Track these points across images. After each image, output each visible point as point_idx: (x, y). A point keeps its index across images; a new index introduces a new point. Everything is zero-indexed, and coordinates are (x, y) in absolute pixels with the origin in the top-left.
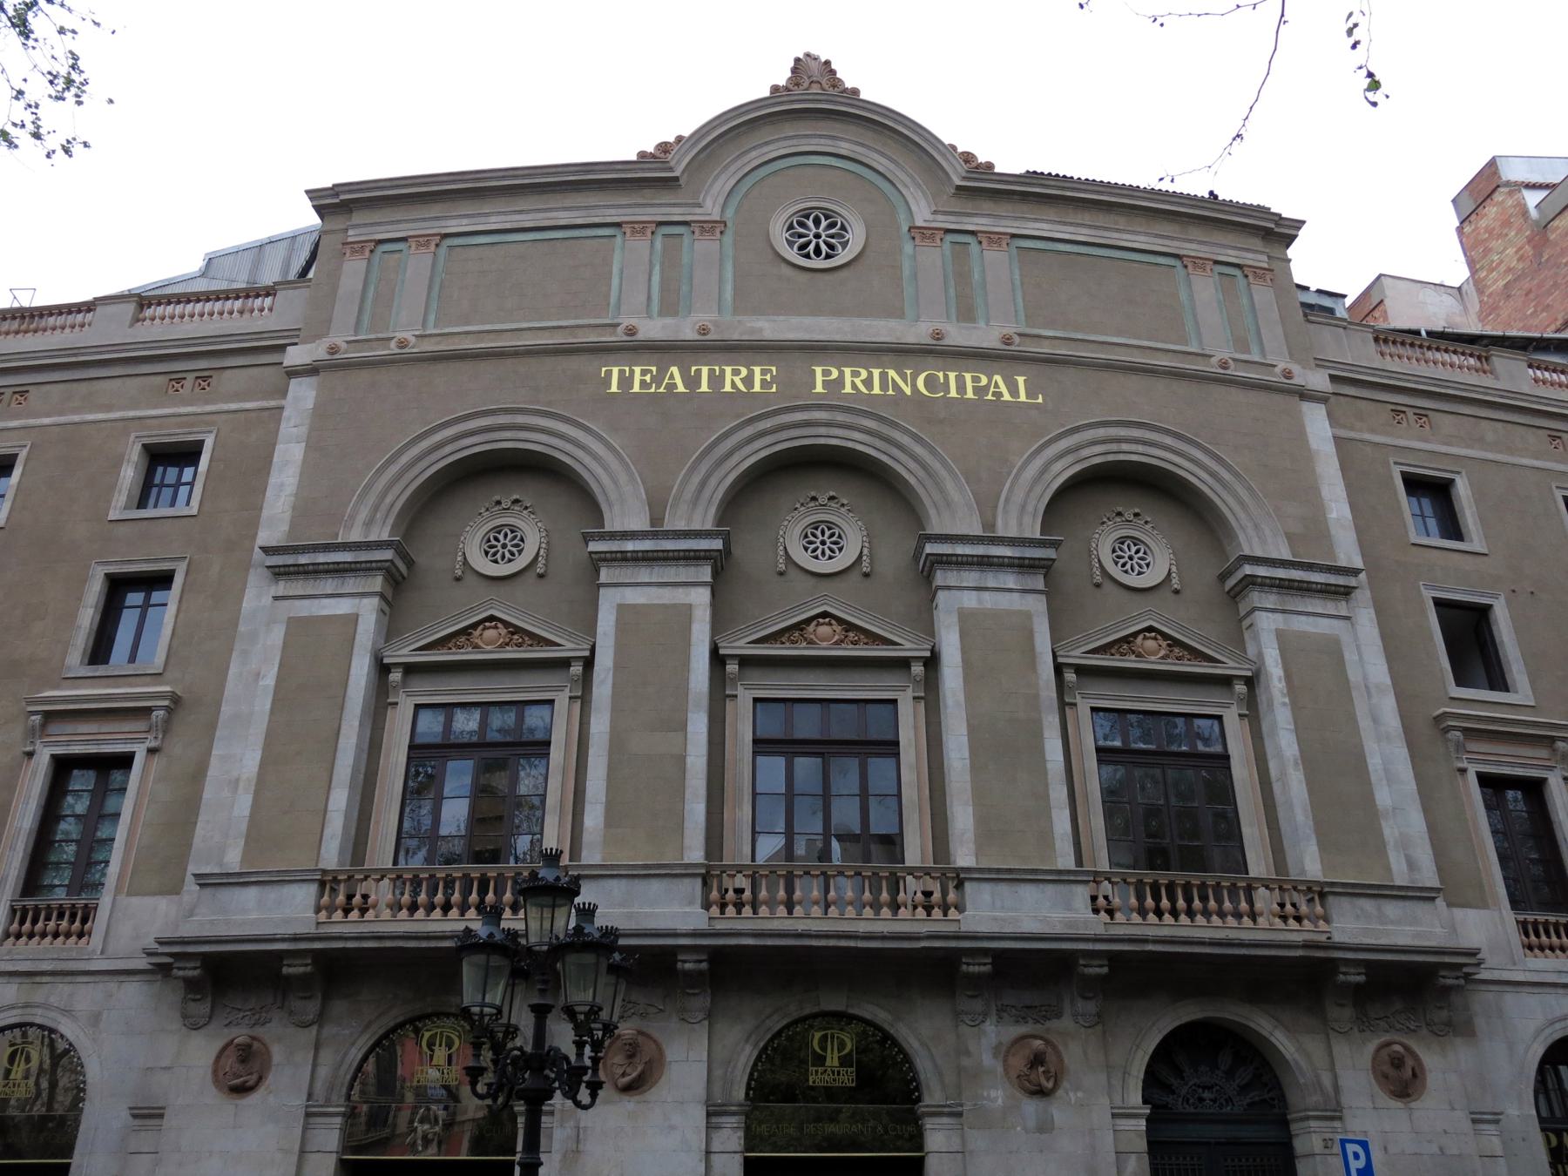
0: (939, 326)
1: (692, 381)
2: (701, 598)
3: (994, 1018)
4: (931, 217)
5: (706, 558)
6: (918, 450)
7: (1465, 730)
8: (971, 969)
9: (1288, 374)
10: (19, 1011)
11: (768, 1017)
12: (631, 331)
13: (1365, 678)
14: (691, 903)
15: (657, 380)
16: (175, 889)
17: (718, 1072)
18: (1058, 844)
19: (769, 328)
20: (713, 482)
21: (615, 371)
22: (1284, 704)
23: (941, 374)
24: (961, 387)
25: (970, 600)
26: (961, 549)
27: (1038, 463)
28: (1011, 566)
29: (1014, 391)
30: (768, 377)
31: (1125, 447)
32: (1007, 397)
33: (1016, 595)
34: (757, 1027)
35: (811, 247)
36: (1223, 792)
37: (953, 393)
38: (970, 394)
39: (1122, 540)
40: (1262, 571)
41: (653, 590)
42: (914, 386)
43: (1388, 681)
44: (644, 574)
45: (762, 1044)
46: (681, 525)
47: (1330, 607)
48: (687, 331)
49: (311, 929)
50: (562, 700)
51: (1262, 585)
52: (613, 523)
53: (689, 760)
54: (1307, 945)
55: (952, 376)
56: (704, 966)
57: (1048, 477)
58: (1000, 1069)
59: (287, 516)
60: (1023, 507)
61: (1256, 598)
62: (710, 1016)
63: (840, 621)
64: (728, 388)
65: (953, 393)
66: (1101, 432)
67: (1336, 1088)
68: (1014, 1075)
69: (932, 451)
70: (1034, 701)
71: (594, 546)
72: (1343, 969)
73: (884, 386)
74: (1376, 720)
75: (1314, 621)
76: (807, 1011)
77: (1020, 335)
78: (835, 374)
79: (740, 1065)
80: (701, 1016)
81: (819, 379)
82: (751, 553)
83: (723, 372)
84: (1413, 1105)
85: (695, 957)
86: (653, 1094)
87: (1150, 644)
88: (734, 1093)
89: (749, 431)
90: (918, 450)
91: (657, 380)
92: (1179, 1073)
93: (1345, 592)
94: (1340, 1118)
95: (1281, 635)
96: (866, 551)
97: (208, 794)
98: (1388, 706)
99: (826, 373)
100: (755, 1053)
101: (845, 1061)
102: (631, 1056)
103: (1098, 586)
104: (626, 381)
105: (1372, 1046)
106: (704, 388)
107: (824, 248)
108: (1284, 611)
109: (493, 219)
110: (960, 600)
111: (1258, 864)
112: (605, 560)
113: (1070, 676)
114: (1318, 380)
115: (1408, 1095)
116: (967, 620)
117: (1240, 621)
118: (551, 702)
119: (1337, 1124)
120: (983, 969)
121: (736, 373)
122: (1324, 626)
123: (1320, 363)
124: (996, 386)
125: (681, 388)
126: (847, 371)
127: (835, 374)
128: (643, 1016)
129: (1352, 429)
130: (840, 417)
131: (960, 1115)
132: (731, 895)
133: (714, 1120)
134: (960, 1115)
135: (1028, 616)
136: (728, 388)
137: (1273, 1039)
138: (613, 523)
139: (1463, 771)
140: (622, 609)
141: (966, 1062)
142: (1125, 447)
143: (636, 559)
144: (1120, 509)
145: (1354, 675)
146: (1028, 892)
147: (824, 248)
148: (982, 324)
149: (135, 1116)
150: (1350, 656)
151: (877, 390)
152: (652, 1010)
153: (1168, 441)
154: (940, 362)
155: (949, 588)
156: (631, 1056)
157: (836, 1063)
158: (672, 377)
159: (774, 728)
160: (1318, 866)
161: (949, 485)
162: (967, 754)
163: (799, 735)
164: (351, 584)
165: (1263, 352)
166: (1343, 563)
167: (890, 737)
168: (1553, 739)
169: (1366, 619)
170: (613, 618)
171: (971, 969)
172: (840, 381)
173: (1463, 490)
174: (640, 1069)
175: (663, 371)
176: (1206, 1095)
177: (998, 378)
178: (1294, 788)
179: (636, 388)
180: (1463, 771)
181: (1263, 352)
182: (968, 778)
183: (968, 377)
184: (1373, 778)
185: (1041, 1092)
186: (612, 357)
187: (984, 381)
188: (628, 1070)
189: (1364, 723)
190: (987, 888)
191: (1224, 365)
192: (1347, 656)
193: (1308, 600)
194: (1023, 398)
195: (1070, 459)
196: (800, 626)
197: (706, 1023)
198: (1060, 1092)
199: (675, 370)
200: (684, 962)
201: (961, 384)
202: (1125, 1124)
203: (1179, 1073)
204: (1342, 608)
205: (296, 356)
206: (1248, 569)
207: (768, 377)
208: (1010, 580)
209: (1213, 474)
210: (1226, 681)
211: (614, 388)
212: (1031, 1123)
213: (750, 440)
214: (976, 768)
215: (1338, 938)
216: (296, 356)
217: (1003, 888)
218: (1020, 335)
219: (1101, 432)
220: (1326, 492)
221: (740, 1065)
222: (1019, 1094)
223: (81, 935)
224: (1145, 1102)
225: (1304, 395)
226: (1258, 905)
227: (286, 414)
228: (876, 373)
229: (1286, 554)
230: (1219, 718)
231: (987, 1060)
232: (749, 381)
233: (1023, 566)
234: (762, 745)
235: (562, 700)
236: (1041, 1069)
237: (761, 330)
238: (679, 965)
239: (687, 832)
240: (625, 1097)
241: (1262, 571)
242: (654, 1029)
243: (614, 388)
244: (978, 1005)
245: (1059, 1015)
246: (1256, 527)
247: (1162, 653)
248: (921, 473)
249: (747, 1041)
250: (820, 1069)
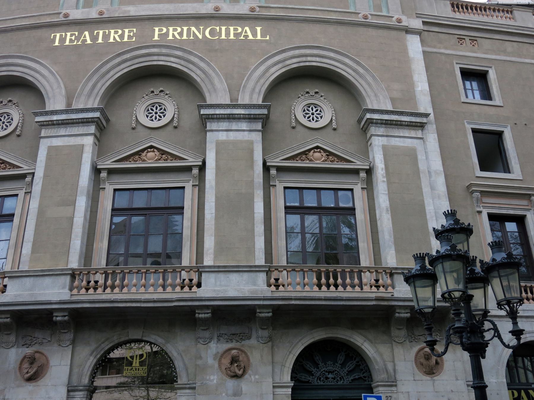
0: (218, 4)
1: (94, 38)
2: (89, 141)
3: (216, 340)
5: (92, 122)
6: (202, 65)
7: (481, 192)
8: (200, 316)
9: (399, 21)
11: (103, 343)
12: (66, 16)
13: (429, 168)
14: (64, 288)
15: (78, 39)
17: (76, 370)
18: (257, 253)
19: (133, 10)
20: (99, 85)
22: (384, 181)
23: (218, 28)
24: (228, 33)
25: (222, 136)
26: (218, 111)
27: (262, 68)
28: (244, 118)
29: (254, 34)
30: (132, 34)
31: (309, 59)
32: (251, 37)
33: (246, 133)
34: (97, 348)
37: (223, 37)
38: (232, 37)
39: (309, 105)
40: (376, 116)
41: (66, 138)
42: (204, 34)
43: (441, 169)
44: (62, 131)
45: (98, 356)
46: (81, 106)
47: (412, 133)
48: (93, 14)
50: (21, 194)
51: (376, 123)
52: (50, 107)
53: (75, 219)
54: (377, 299)
55: (224, 28)
56: (66, 318)
57: (268, 75)
58: (216, 365)
60: (254, 89)
61: (373, 130)
62: (73, 343)
63: (159, 150)
64: (111, 40)
65: (223, 37)
66: (297, 52)
67: (395, 371)
68: (223, 368)
69: (208, 64)
70: (251, 184)
71: (38, 119)
72: (398, 311)
73: (188, 35)
74: (432, 188)
75: (403, 140)
76: (123, 339)
77: (259, 7)
79: (87, 367)
80: (68, 343)
81: (157, 33)
82: (119, 119)
83: (110, 33)
84: (435, 378)
85: (62, 314)
86: (41, 382)
87: (317, 155)
88: (83, 381)
89: (118, 60)
90: (202, 65)
91: (78, 39)
92: (316, 365)
93: (421, 126)
94: (396, 386)
95: (385, 148)
96: (176, 116)
98: (440, 182)
99: (160, 30)
100: (95, 361)
101: (142, 364)
102: (32, 363)
103: (294, 128)
105: (416, 349)
106: (100, 41)
108: (387, 136)
110: (218, 135)
111: (365, 260)
112: (43, 125)
113: (273, 172)
114: (417, 24)
115: (434, 373)
116: (220, 146)
117: (367, 142)
118: (17, 195)
119: (394, 389)
120: (206, 315)
121: (116, 32)
122: (408, 143)
123: (418, 16)
124: (246, 32)
125: (89, 42)
126: (171, 29)
127: (165, 30)
128: (41, 344)
129: (435, 47)
130: (164, 51)
131: (194, 388)
132: (92, 283)
133: (71, 394)
134: (194, 388)
135: (251, 143)
136: (111, 40)
137: (363, 347)
138: (50, 107)
139: (480, 212)
140: (50, 148)
141: (199, 362)
142: (309, 59)
143: (59, 124)
144: (308, 90)
145: (422, 166)
146: (234, 277)
148: (242, 3)
150: (421, 157)
151: (185, 37)
152: (44, 341)
153: (332, 55)
154: (218, 22)
155: (212, 131)
156: (32, 363)
157: (138, 364)
158: (85, 36)
159: (123, 202)
160: (395, 261)
161: (216, 81)
162: (214, 211)
163: (135, 206)
165: (388, 11)
166: (422, 110)
167: (180, 205)
168: (530, 195)
169: (432, 138)
170: (45, 153)
171: (200, 316)
172: (167, 34)
173: (492, 76)
174: (34, 370)
175: (81, 34)
176: (330, 376)
177: (247, 28)
178: (385, 222)
179: (67, 43)
180: (480, 212)
181: (388, 11)
182: (213, 222)
183: (232, 28)
184: (428, 217)
185: (236, 376)
186: (57, 29)
187: (240, 30)
188: (30, 371)
189: (426, 190)
190: (213, 275)
191: (365, 17)
192: (419, 157)
193: (401, 131)
194: (259, 37)
195: (280, 65)
196: (139, 153)
197: (71, 346)
198: (246, 376)
199: (87, 33)
200: (57, 316)
201: (227, 32)
202: (279, 391)
203: (316, 365)
204: (419, 134)
206: (368, 116)
207: (132, 34)
208: (244, 125)
209: (355, 71)
210: (356, 172)
212: (230, 392)
213: (119, 64)
214: (217, 218)
215: (396, 295)
217: (221, 276)
218: (259, 7)
219: (297, 52)
220: (416, 78)
221: (87, 367)
222: (224, 377)
224: (292, 380)
225: (408, 31)
226: (364, 280)
228: (185, 29)
229: (390, 108)
230: (352, 190)
231: (210, 361)
232: (122, 36)
233: (251, 118)
234: (115, 211)
235: (21, 194)
236: (236, 365)
237: (129, 11)
238: (54, 318)
239: (71, 254)
240: (28, 384)
241: (376, 116)
242: (45, 349)
243: (57, 44)
244: (207, 334)
245: (249, 338)
246: (376, 95)
247: (323, 159)
248: (203, 76)
249: (91, 355)
250: (130, 368)
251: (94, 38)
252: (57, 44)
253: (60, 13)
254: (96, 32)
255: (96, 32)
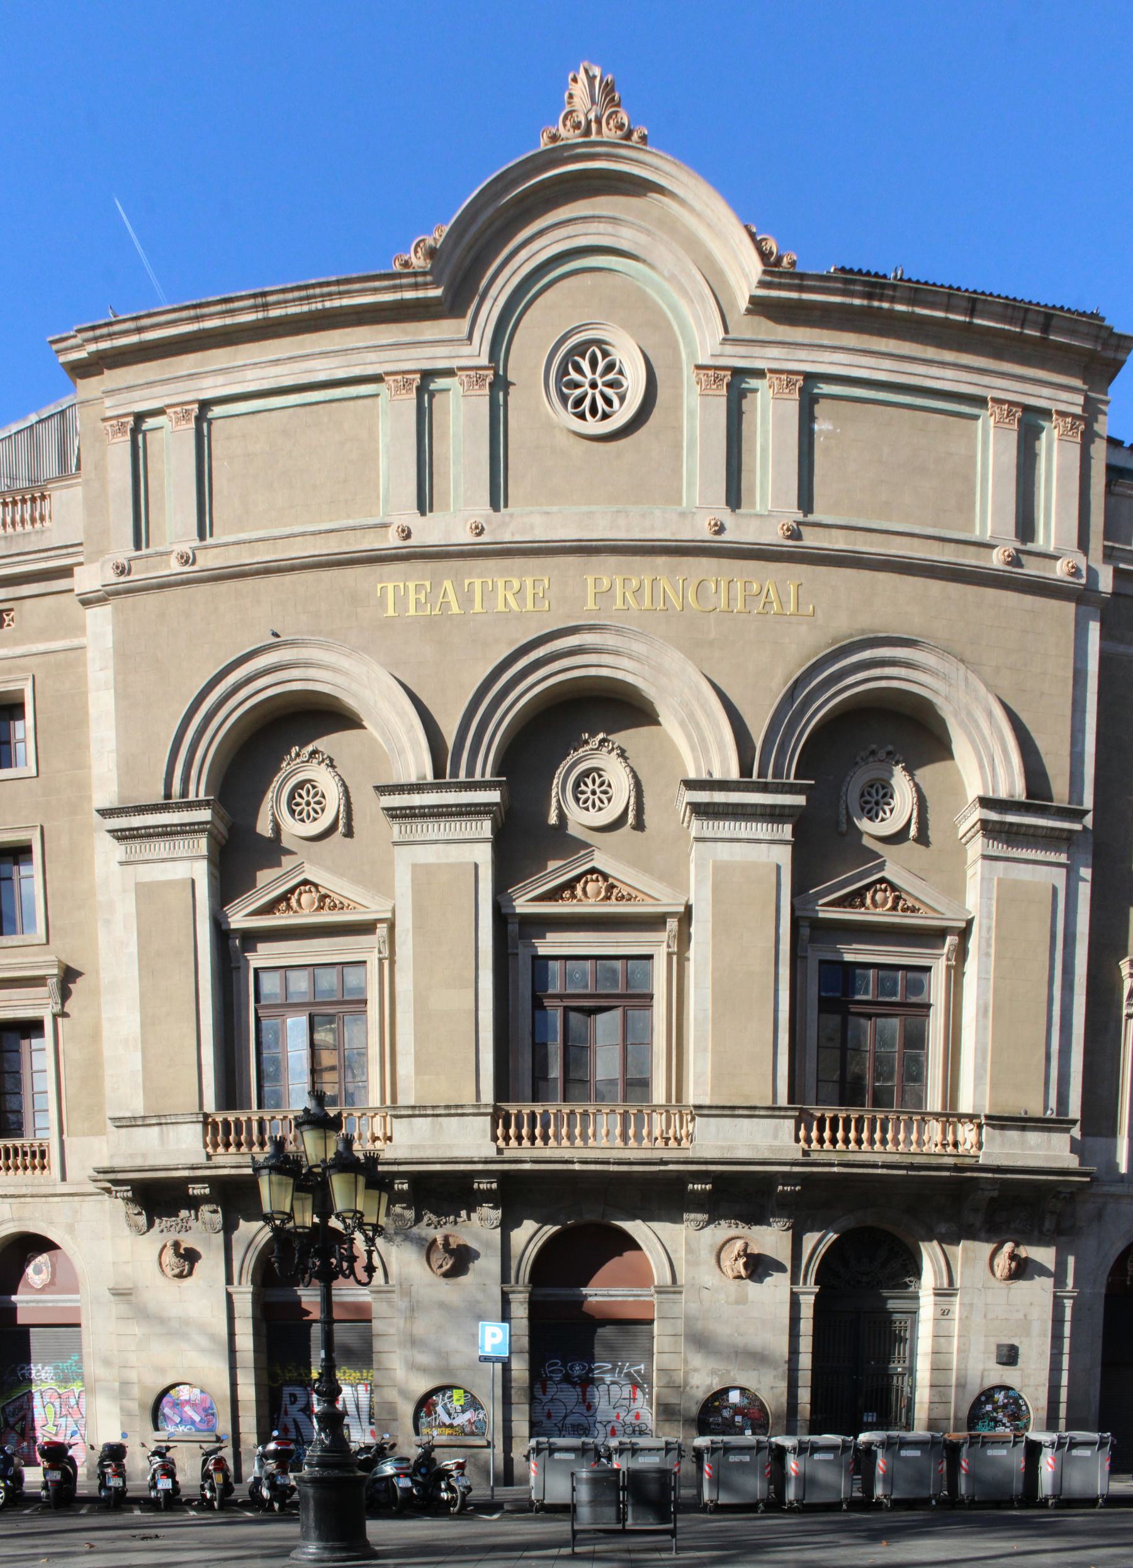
1: (466, 599)
4: (718, 349)
10: (16, 1223)
16: (101, 1132)
21: (390, 587)
35: (587, 403)
36: (916, 1040)
49: (202, 1160)
59: (114, 775)
78: (606, 583)
83: (494, 589)
97: (107, 1051)
104: (401, 601)
106: (478, 607)
107: (600, 404)
109: (250, 374)
125: (455, 609)
127: (606, 583)
136: (501, 607)
143: (424, 816)
147: (600, 404)
149: (114, 1294)
151: (647, 603)
164: (182, 846)
179: (412, 611)
199: (448, 584)
205: (88, 579)
211: (391, 612)
216: (88, 579)
223: (43, 1168)
227: (90, 654)
251: (466, 599)
252: (391, 612)
253: (385, 526)
254: (467, 582)
255: (467, 582)
